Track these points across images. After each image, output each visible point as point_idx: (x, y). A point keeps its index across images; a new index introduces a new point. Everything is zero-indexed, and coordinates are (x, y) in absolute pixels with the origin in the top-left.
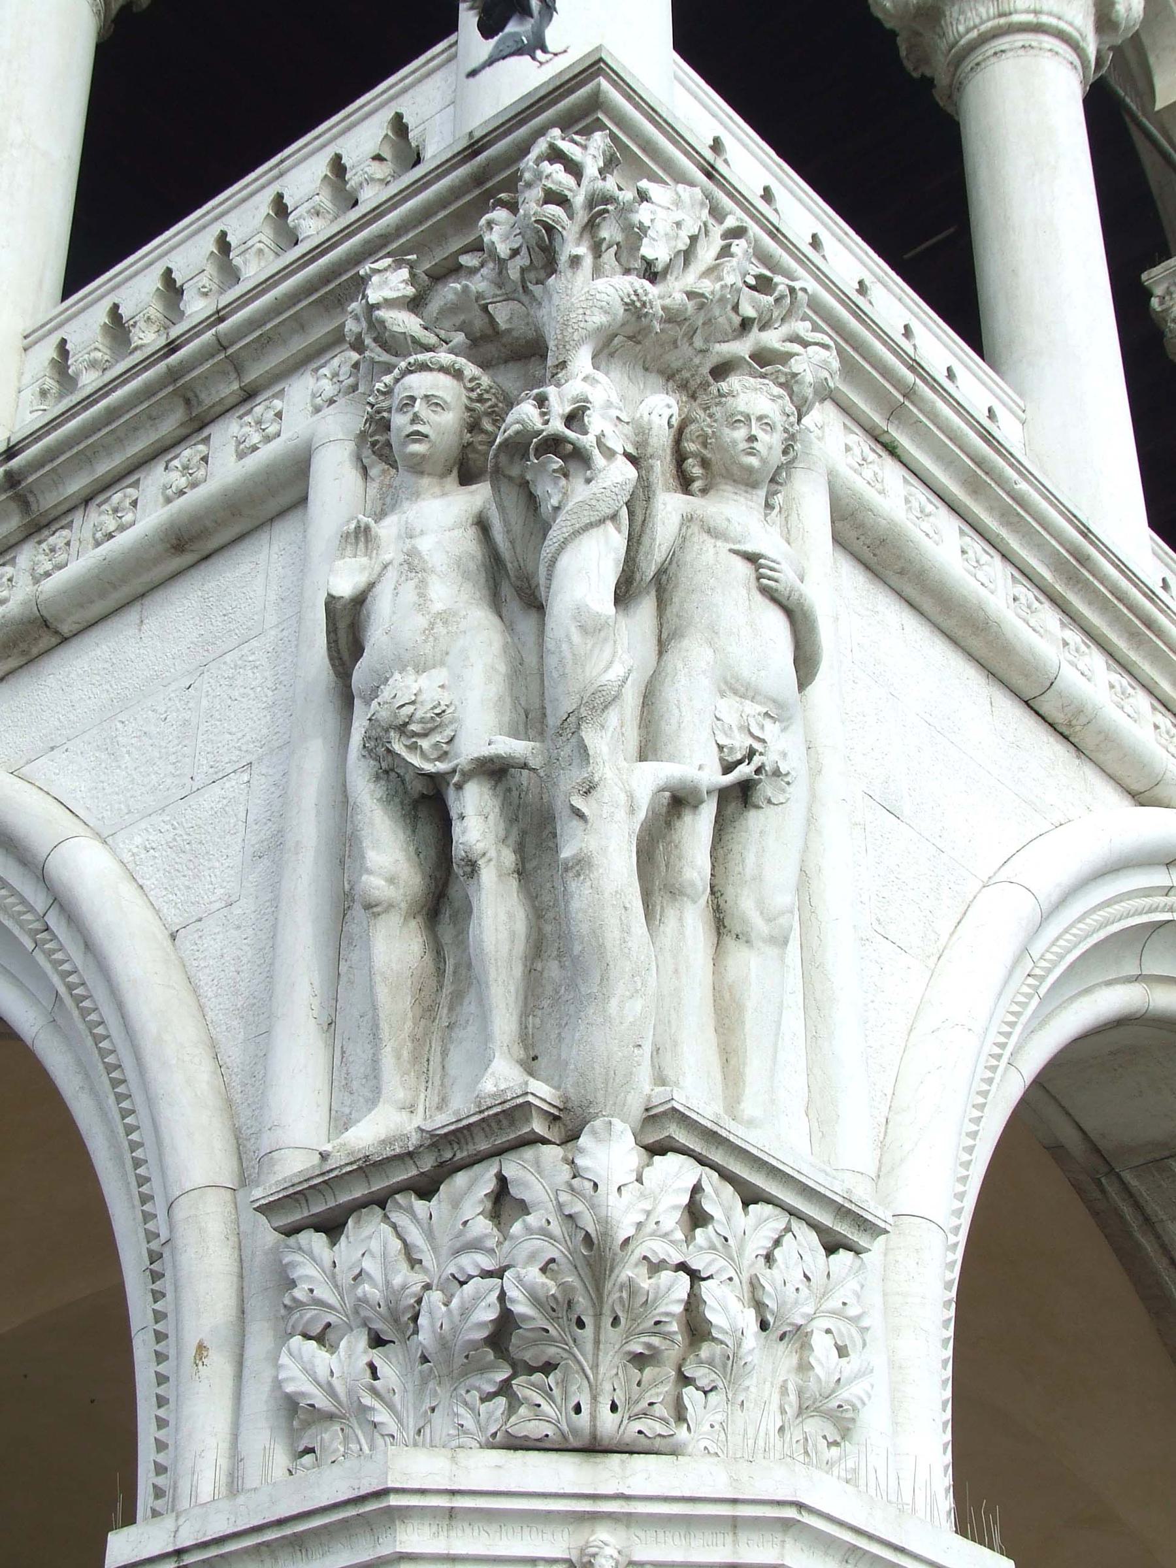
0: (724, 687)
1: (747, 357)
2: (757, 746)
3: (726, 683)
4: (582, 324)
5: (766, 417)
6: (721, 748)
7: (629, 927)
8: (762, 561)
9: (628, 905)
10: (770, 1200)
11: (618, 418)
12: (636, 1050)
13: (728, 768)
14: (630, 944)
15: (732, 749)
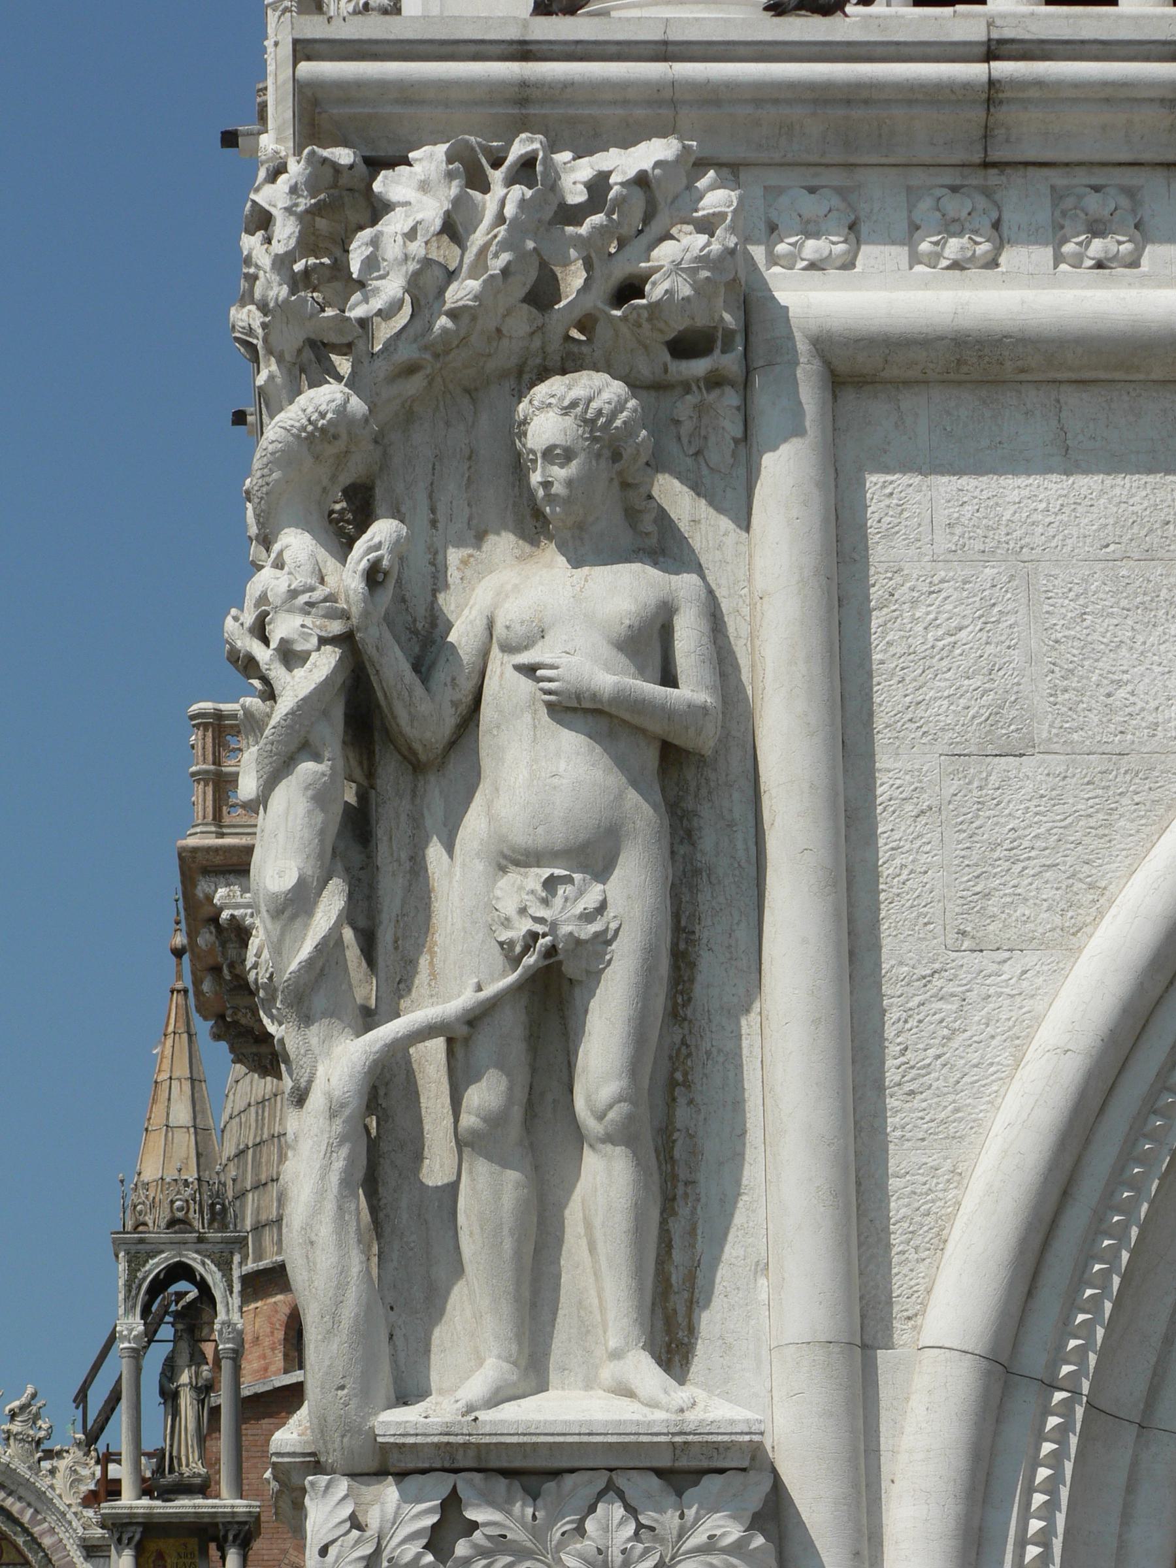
0: (504, 862)
1: (600, 305)
2: (540, 929)
3: (505, 857)
4: (264, 489)
5: (555, 446)
6: (501, 944)
7: (315, 1264)
8: (539, 673)
9: (314, 1238)
10: (572, 1471)
11: (311, 604)
12: (339, 1392)
13: (516, 961)
14: (316, 1284)
15: (511, 943)
